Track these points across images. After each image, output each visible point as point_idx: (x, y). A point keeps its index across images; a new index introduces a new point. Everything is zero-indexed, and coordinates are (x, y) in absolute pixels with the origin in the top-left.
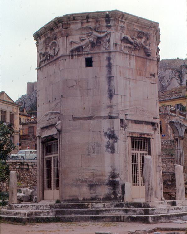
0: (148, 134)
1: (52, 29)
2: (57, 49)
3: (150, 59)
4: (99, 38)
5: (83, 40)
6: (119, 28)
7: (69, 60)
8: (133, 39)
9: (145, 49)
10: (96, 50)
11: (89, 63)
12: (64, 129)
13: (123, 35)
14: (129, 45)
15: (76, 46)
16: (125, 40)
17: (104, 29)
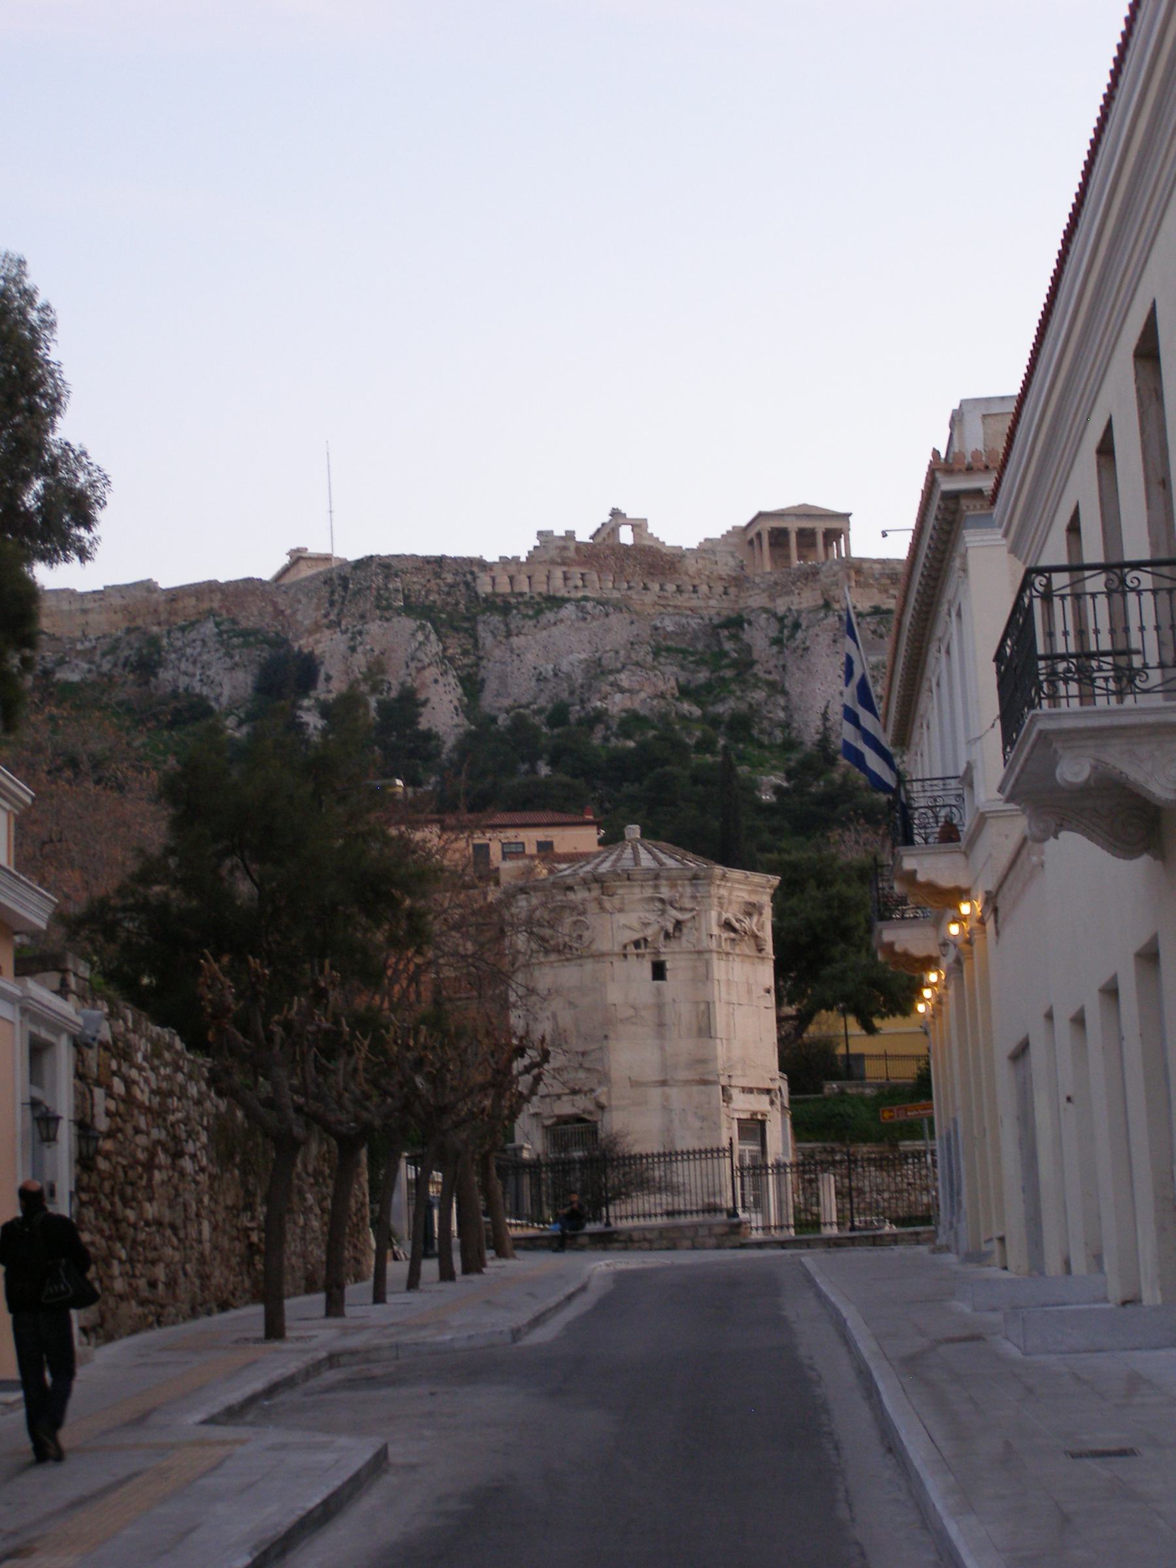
0: (763, 1114)
1: (570, 888)
2: (587, 935)
3: (763, 958)
4: (678, 924)
5: (646, 925)
6: (715, 901)
7: (618, 964)
8: (738, 920)
9: (756, 937)
10: (674, 945)
11: (659, 971)
12: (614, 1103)
13: (725, 916)
14: (732, 935)
15: (636, 936)
16: (728, 926)
17: (688, 905)
